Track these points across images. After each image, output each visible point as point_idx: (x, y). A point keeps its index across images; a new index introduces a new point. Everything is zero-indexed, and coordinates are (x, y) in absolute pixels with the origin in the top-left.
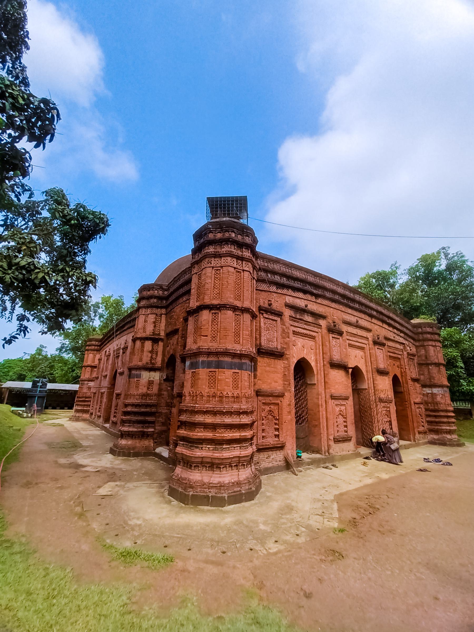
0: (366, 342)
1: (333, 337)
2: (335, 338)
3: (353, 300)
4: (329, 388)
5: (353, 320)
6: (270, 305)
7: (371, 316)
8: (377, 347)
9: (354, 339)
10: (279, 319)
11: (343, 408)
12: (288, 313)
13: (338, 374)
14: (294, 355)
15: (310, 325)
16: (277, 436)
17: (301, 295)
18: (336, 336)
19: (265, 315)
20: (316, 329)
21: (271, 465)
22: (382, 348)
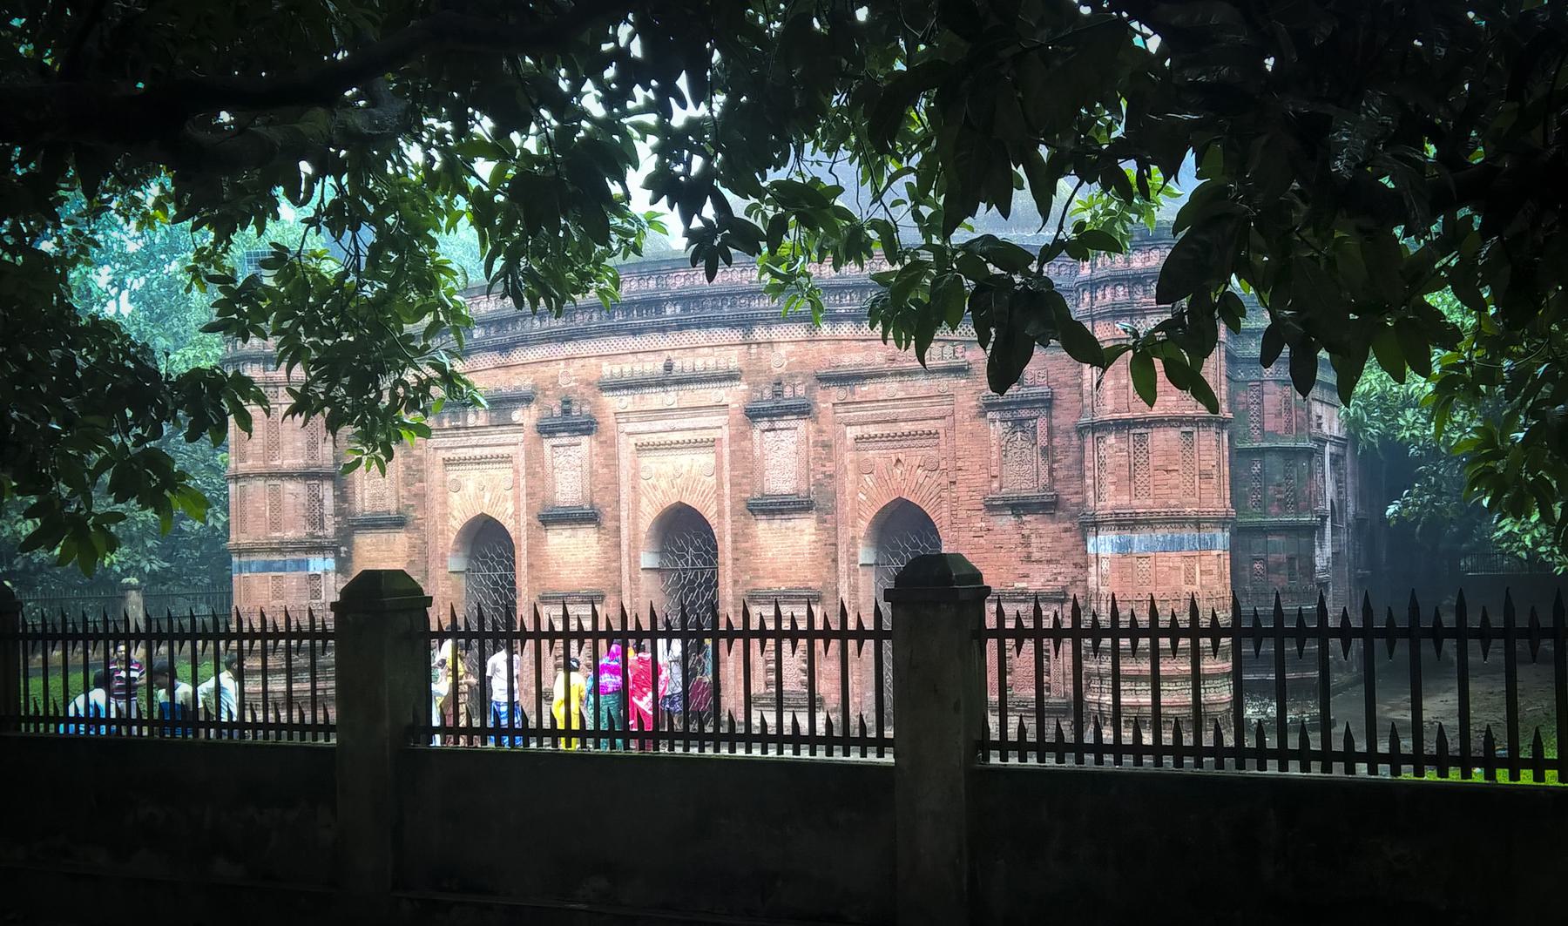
5: (652, 366)
7: (746, 323)
8: (765, 425)
9: (659, 425)
13: (573, 540)
14: (456, 513)
15: (489, 433)
20: (509, 437)
22: (793, 424)
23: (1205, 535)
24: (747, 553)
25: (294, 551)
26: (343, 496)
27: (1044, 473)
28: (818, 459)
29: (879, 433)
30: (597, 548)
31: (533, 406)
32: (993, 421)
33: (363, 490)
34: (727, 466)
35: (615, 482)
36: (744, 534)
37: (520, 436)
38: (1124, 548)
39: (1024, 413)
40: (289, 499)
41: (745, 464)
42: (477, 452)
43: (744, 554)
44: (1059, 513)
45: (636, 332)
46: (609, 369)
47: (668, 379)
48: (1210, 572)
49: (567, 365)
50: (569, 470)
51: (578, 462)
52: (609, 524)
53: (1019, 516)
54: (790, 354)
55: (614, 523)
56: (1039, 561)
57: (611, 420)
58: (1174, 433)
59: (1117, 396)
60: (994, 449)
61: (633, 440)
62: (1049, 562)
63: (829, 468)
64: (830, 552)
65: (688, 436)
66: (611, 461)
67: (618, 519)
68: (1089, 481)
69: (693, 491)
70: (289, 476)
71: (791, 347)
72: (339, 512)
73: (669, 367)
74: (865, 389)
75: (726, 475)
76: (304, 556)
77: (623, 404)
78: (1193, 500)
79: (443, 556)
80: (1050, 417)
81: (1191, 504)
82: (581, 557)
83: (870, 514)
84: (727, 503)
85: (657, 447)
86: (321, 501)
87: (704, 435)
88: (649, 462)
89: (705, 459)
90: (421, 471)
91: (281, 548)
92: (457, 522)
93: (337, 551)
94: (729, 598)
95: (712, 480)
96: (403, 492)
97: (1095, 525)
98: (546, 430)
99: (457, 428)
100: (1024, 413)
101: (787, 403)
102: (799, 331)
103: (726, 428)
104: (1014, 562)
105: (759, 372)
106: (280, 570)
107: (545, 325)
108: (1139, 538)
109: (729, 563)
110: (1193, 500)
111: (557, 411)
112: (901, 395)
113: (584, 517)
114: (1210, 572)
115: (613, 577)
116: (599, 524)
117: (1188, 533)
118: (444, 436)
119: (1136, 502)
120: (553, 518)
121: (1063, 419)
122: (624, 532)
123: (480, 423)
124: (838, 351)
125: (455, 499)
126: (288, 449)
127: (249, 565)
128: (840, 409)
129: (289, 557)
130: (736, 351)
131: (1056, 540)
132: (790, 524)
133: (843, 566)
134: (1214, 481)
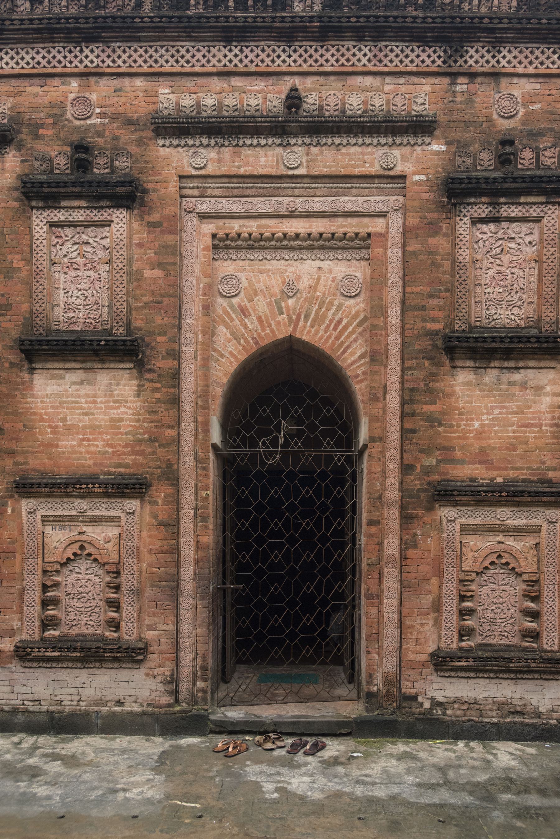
1: (52, 225)
2: (72, 225)
4: (12, 453)
5: (262, 97)
8: (482, 211)
13: (86, 389)
18: (79, 216)
22: (534, 212)
24: (433, 421)
34: (394, 276)
36: (429, 391)
46: (169, 98)
47: (292, 123)
51: (102, 254)
52: (162, 364)
55: (171, 363)
57: (172, 188)
61: (208, 228)
65: (319, 226)
66: (170, 258)
67: (176, 355)
69: (318, 320)
73: (294, 100)
75: (393, 294)
77: (199, 161)
82: (102, 418)
84: (395, 338)
87: (351, 226)
88: (236, 269)
89: (340, 269)
95: (357, 306)
111: (61, 162)
132: (517, 376)
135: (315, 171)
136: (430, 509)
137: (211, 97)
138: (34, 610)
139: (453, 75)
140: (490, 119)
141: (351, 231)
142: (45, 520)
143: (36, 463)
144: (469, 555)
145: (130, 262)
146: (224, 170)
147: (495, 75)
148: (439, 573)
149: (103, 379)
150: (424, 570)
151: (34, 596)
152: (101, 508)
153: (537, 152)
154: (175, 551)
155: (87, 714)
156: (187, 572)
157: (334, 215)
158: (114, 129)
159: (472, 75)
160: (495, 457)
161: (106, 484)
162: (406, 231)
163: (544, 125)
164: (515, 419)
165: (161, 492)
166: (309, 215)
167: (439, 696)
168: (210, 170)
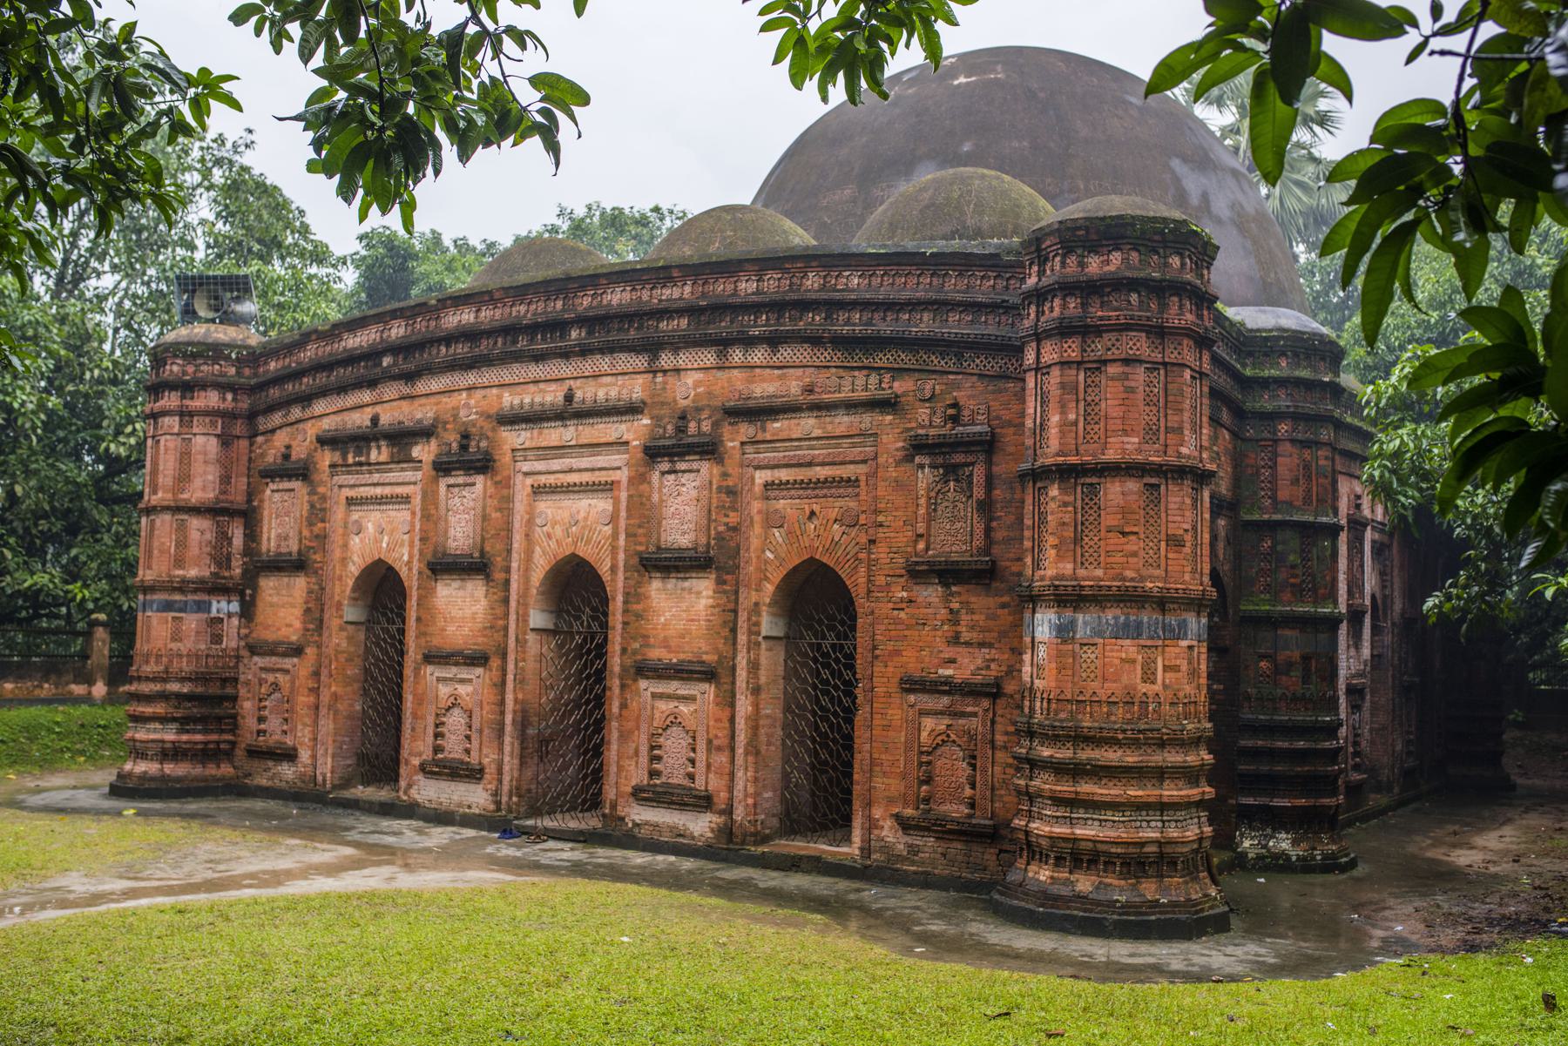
0: (617, 459)
3: (557, 326)
5: (552, 396)
6: (286, 457)
7: (651, 348)
8: (666, 466)
9: (556, 464)
10: (296, 484)
11: (463, 690)
12: (326, 458)
13: (461, 593)
14: (355, 558)
15: (390, 470)
16: (285, 732)
17: (366, 396)
18: (460, 480)
19: (272, 486)
20: (409, 475)
21: (270, 783)
23: (1172, 620)
24: (639, 616)
25: (195, 591)
26: (252, 535)
27: (979, 529)
28: (721, 507)
29: (791, 479)
30: (484, 602)
31: (434, 442)
32: (922, 466)
33: (270, 529)
34: (623, 514)
35: (509, 529)
37: (419, 475)
38: (1064, 632)
39: (959, 458)
40: (194, 535)
41: (643, 513)
42: (379, 491)
43: (635, 617)
44: (995, 585)
45: (539, 358)
46: (509, 400)
47: (569, 412)
48: (1176, 669)
49: (469, 396)
50: (462, 514)
51: (472, 504)
52: (499, 576)
53: (946, 585)
54: (697, 384)
55: (503, 575)
56: (968, 644)
57: (508, 458)
58: (1133, 485)
59: (1062, 434)
60: (922, 501)
61: (529, 481)
62: (981, 645)
63: (733, 518)
64: (729, 618)
65: (586, 477)
67: (508, 570)
68: (1027, 544)
69: (588, 542)
70: (196, 510)
71: (699, 376)
72: (248, 551)
73: (569, 398)
74: (777, 426)
75: (622, 523)
76: (206, 598)
77: (520, 440)
78: (1157, 572)
79: (339, 605)
80: (989, 463)
81: (1152, 578)
82: (468, 612)
83: (777, 576)
84: (621, 556)
85: (554, 490)
86: (230, 541)
88: (548, 508)
89: (599, 505)
90: (324, 510)
91: (183, 586)
92: (354, 569)
93: (242, 594)
94: (617, 669)
95: (608, 530)
96: (306, 533)
97: (1032, 600)
98: (442, 467)
99: (360, 464)
100: (959, 458)
101: (690, 440)
102: (708, 357)
103: (625, 470)
104: (940, 643)
105: (663, 404)
106: (180, 611)
107: (451, 351)
108: (1084, 621)
109: (619, 626)
110: (1157, 572)
111: (455, 445)
112: (817, 433)
113: (473, 566)
114: (1176, 669)
115: (498, 636)
116: (488, 578)
117: (1147, 617)
118: (349, 473)
119: (1081, 572)
120: (444, 566)
121: (1004, 467)
122: (514, 586)
123: (384, 457)
124: (750, 381)
125: (355, 541)
126: (198, 482)
127: (152, 602)
128: (749, 449)
129: (190, 597)
130: (640, 379)
131: (992, 617)
132: (687, 584)
133: (742, 638)
134: (1187, 550)
135: (581, 442)
136: (635, 680)
137: (529, 398)
138: (430, 739)
139: (655, 372)
140: (675, 401)
141: (603, 480)
142: (439, 680)
143: (436, 641)
144: (657, 715)
145: (484, 508)
146: (534, 444)
147: (677, 371)
148: (638, 728)
149: (470, 585)
150: (631, 725)
151: (430, 730)
152: (464, 673)
153: (699, 422)
154: (502, 702)
155: (453, 812)
156: (509, 718)
157: (593, 470)
158: (481, 422)
159: (665, 372)
160: (673, 643)
161: (466, 657)
162: (631, 480)
163: (705, 402)
164: (684, 615)
165: (495, 663)
166: (580, 470)
167: (637, 819)
168: (527, 445)
